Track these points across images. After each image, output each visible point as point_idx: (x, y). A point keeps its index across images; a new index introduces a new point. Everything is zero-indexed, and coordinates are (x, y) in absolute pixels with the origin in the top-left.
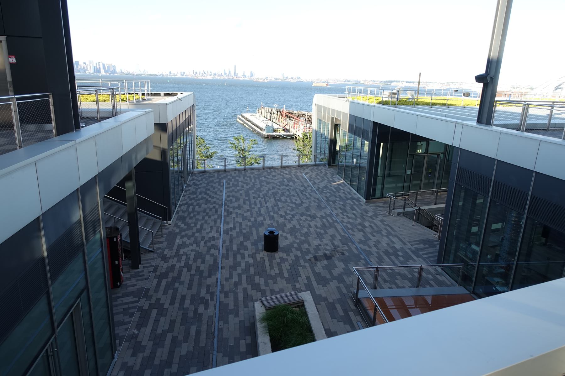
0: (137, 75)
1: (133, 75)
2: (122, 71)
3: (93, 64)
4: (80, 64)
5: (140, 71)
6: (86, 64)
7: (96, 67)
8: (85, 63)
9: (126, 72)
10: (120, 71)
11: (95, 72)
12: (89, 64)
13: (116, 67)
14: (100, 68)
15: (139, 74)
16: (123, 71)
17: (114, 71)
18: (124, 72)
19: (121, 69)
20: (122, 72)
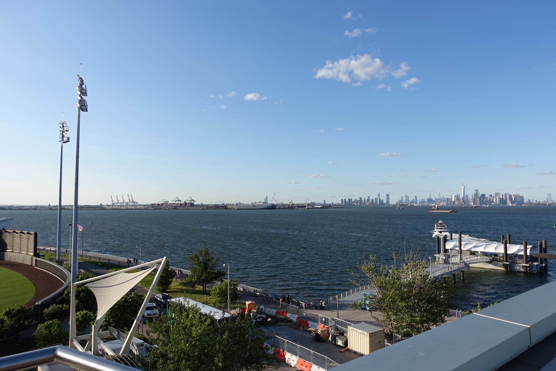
0: (549, 205)
1: (545, 205)
2: (530, 201)
3: (499, 196)
4: (486, 197)
5: (553, 201)
6: (492, 197)
7: (503, 198)
8: (491, 196)
9: (536, 202)
10: (528, 201)
11: (501, 204)
12: (494, 196)
13: (523, 197)
14: (506, 199)
15: (552, 204)
16: (531, 201)
17: (522, 202)
18: (532, 203)
19: (529, 200)
20: (529, 203)
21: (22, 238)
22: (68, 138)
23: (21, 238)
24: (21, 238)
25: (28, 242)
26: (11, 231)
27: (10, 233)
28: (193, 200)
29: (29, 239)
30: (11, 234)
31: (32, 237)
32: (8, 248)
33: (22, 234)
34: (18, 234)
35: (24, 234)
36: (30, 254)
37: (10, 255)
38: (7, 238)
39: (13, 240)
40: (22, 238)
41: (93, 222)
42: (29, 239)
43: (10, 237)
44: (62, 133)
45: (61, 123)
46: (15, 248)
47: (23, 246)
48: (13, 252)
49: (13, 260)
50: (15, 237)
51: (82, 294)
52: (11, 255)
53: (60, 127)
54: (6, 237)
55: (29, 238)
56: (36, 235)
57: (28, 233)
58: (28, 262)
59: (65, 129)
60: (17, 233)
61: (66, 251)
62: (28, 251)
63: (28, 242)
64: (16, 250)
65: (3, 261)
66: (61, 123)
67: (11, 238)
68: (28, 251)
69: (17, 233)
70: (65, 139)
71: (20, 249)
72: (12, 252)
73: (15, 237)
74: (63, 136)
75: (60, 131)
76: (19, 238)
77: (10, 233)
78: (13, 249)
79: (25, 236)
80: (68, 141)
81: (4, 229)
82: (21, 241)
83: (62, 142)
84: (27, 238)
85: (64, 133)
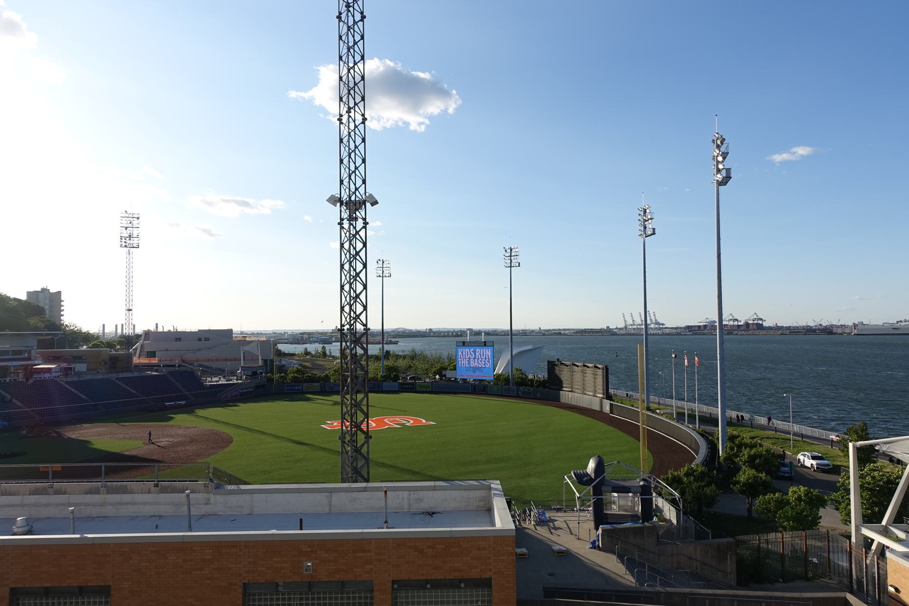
21: (585, 373)
22: (654, 229)
23: (584, 373)
24: (584, 373)
25: (595, 379)
26: (569, 363)
27: (567, 366)
28: (761, 319)
29: (597, 375)
30: (568, 367)
31: (600, 372)
32: (564, 385)
33: (586, 368)
34: (580, 368)
35: (588, 367)
36: (599, 395)
37: (566, 396)
38: (563, 372)
39: (572, 375)
40: (585, 373)
41: (618, 354)
42: (597, 375)
43: (568, 371)
44: (644, 224)
45: (640, 209)
46: (576, 387)
47: (588, 385)
48: (574, 392)
49: (573, 403)
50: (574, 372)
51: (758, 461)
52: (570, 396)
53: (639, 215)
54: (562, 371)
55: (597, 373)
56: (606, 370)
57: (596, 367)
58: (596, 407)
59: (649, 217)
60: (577, 366)
61: (627, 394)
62: (595, 391)
63: (595, 379)
64: (577, 389)
65: (559, 403)
66: (640, 209)
67: (569, 373)
68: (595, 391)
69: (577, 366)
70: (649, 232)
71: (584, 389)
72: (571, 391)
73: (574, 372)
74: (645, 228)
75: (639, 220)
76: (580, 373)
77: (567, 366)
78: (572, 387)
79: (589, 371)
80: (654, 233)
81: (558, 360)
82: (584, 377)
83: (644, 236)
84: (593, 374)
85: (646, 223)
